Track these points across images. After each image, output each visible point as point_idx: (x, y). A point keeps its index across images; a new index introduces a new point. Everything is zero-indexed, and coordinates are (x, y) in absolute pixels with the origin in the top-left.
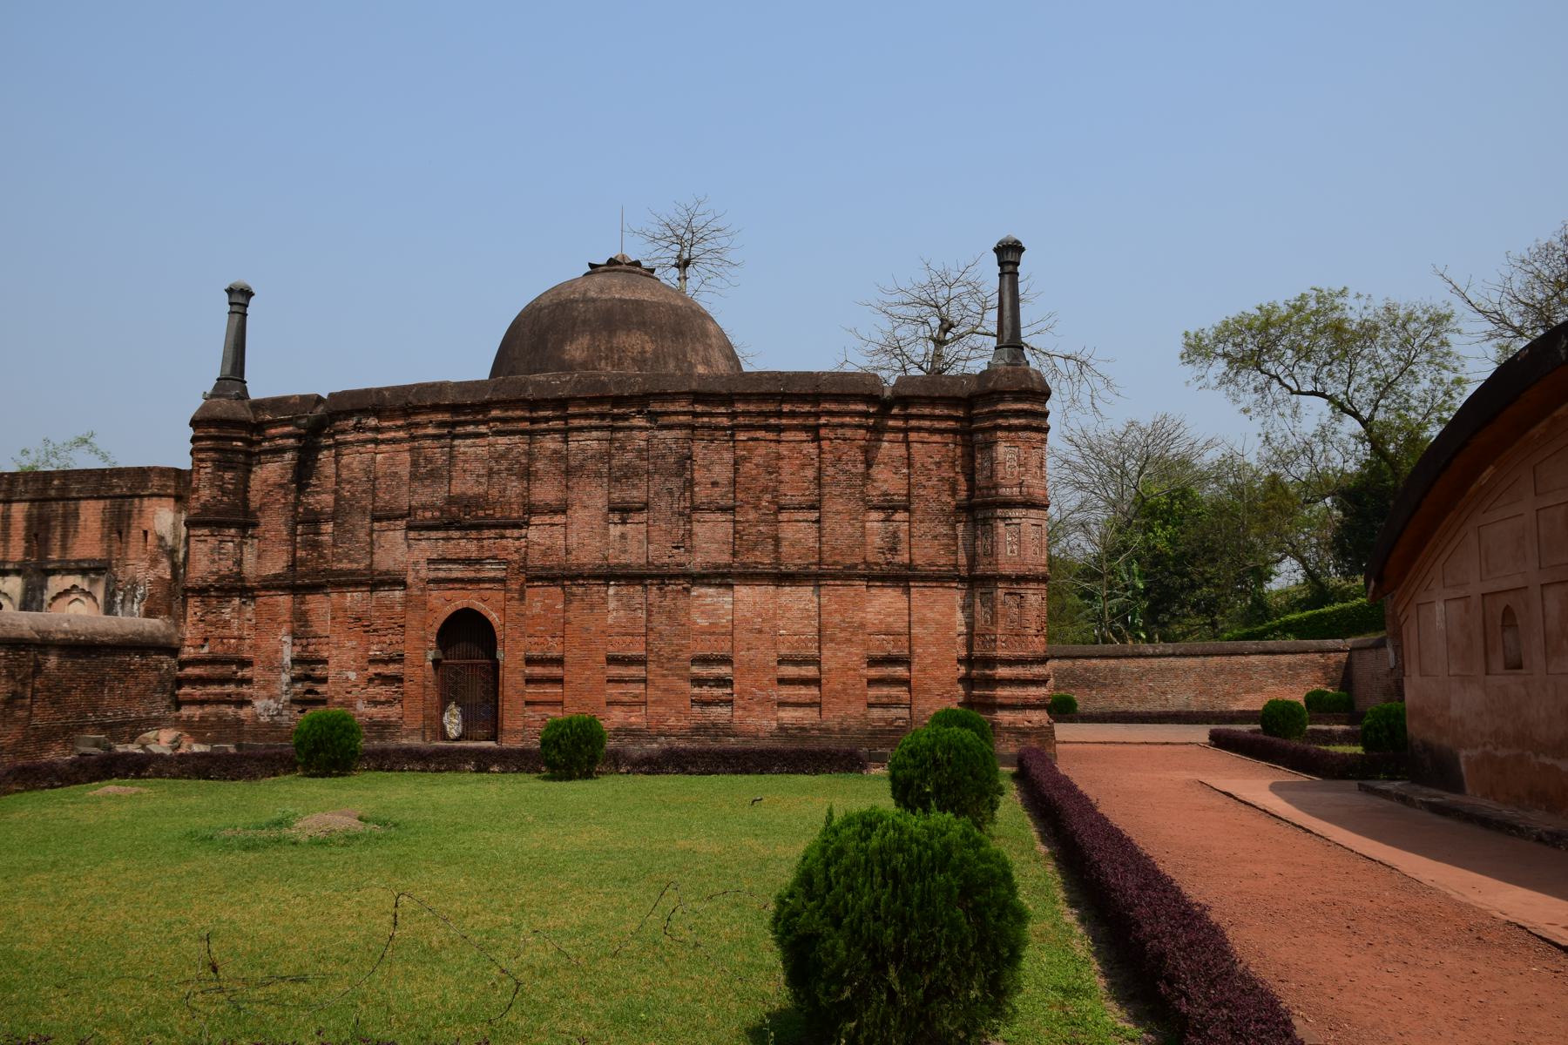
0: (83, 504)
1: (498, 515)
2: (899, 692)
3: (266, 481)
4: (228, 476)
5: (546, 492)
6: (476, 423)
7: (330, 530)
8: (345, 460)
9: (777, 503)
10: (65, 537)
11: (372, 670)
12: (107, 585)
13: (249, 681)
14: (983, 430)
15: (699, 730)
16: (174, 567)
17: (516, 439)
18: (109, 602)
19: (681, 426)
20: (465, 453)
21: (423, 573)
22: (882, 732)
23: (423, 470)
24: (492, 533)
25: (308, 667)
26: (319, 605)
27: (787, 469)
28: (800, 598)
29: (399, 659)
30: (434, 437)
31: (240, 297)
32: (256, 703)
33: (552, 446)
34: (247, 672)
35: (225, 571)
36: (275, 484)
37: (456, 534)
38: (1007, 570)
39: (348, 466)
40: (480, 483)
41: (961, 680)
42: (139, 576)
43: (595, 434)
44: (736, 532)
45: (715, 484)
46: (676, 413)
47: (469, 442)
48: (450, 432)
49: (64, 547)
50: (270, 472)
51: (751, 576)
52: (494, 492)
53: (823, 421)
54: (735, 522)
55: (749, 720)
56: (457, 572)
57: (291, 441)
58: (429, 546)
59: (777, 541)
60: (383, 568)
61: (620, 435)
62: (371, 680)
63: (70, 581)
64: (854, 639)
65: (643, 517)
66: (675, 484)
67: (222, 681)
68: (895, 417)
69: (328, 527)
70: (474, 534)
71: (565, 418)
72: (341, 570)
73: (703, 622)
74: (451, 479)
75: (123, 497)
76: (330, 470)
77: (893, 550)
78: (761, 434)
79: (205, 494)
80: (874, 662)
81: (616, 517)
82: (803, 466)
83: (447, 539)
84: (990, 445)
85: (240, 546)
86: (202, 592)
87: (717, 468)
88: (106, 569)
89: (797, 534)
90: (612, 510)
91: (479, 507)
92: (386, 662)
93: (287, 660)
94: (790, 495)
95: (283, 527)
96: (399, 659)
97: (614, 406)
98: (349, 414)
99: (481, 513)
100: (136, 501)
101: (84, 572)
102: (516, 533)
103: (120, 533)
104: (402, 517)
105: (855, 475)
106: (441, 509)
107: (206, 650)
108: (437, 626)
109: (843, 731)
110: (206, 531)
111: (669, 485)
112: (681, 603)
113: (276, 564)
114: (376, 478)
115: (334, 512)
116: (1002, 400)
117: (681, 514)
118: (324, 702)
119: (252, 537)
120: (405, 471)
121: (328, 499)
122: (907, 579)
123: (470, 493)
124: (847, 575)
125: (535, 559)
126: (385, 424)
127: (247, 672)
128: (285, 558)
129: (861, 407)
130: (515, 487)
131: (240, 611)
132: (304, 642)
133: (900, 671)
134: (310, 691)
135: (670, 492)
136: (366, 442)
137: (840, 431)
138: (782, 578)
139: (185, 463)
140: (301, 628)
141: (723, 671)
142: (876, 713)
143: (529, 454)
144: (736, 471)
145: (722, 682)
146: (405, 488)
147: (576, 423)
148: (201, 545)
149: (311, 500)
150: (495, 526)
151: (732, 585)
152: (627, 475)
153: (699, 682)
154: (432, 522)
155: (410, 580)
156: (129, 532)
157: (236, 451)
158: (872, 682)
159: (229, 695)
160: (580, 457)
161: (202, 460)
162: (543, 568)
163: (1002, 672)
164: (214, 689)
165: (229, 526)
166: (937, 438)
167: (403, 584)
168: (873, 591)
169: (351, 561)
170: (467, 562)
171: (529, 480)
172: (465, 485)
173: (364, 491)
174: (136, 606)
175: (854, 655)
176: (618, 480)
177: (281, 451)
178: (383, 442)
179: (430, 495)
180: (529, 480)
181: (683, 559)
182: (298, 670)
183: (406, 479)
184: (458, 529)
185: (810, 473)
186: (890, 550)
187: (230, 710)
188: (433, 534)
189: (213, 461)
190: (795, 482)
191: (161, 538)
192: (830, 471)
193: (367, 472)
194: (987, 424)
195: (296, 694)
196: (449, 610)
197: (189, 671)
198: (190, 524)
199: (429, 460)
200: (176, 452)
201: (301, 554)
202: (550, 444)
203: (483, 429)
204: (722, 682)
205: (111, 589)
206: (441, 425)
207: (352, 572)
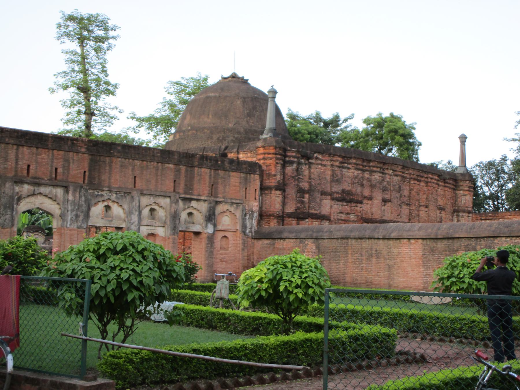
0: (231, 174)
6: (348, 163)
8: (312, 170)
18: (244, 219)
30: (339, 167)
36: (290, 176)
37: (345, 204)
39: (313, 173)
40: (349, 186)
43: (379, 174)
44: (410, 212)
47: (346, 170)
52: (354, 190)
53: (430, 180)
54: (410, 209)
57: (296, 160)
63: (226, 207)
65: (389, 204)
66: (398, 195)
69: (307, 196)
70: (349, 204)
72: (312, 213)
76: (306, 173)
82: (424, 194)
83: (342, 205)
88: (241, 204)
94: (422, 203)
95: (294, 194)
99: (351, 197)
100: (252, 175)
115: (309, 190)
120: (328, 178)
128: (294, 206)
130: (359, 189)
144: (410, 193)
146: (329, 184)
150: (355, 203)
155: (332, 219)
160: (375, 181)
161: (277, 163)
169: (315, 210)
172: (347, 186)
173: (318, 184)
174: (254, 221)
189: (281, 164)
192: (430, 196)
201: (299, 205)
203: (350, 166)
205: (244, 212)
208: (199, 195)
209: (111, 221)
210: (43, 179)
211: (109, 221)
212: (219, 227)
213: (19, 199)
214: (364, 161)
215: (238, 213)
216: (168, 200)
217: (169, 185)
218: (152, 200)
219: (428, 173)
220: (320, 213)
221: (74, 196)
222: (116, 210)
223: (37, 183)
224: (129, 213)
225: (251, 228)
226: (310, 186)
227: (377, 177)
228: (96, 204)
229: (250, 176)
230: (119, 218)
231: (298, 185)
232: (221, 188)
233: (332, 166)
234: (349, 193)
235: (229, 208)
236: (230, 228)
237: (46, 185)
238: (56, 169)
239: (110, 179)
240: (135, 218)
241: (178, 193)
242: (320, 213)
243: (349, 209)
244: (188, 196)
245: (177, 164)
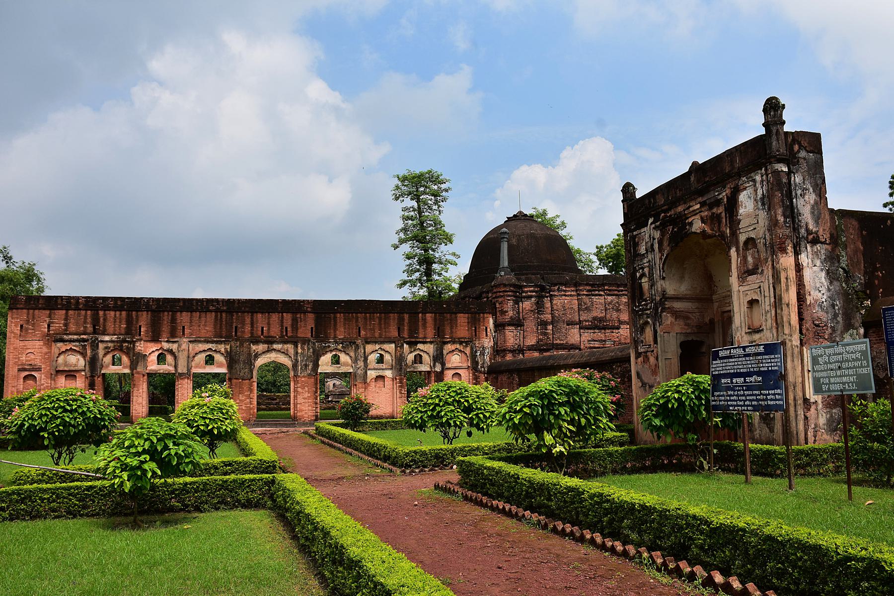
0: (459, 315)
6: (599, 291)
7: (551, 328)
8: (554, 302)
10: (451, 328)
12: (472, 349)
20: (596, 301)
23: (583, 307)
30: (587, 295)
42: (486, 345)
47: (597, 297)
49: (452, 332)
57: (534, 293)
58: (587, 335)
69: (550, 327)
70: (603, 331)
75: (476, 313)
76: (548, 305)
79: (511, 313)
99: (605, 324)
100: (482, 315)
101: (461, 343)
103: (475, 328)
104: (577, 324)
113: (531, 341)
120: (576, 307)
130: (615, 315)
146: (577, 313)
150: (610, 329)
154: (589, 327)
155: (582, 347)
156: (479, 327)
161: (509, 300)
167: (580, 349)
170: (601, 341)
172: (598, 313)
173: (563, 314)
177: (530, 297)
183: (577, 310)
188: (590, 331)
189: (513, 300)
199: (585, 304)
203: (602, 293)
206: (588, 291)
208: (425, 338)
209: (340, 367)
210: (276, 337)
211: (337, 367)
212: (448, 365)
213: (257, 356)
214: (619, 286)
216: (393, 345)
217: (394, 333)
218: (377, 347)
220: (567, 343)
221: (303, 348)
222: (343, 358)
223: (270, 341)
224: (355, 361)
225: (483, 363)
226: (553, 317)
228: (324, 354)
229: (479, 316)
230: (346, 364)
231: (538, 318)
232: (448, 330)
233: (578, 295)
234: (601, 320)
235: (458, 346)
236: (461, 365)
237: (278, 343)
238: (286, 328)
239: (335, 331)
240: (361, 364)
241: (403, 337)
242: (567, 343)
243: (602, 336)
244: (414, 340)
245: (401, 313)
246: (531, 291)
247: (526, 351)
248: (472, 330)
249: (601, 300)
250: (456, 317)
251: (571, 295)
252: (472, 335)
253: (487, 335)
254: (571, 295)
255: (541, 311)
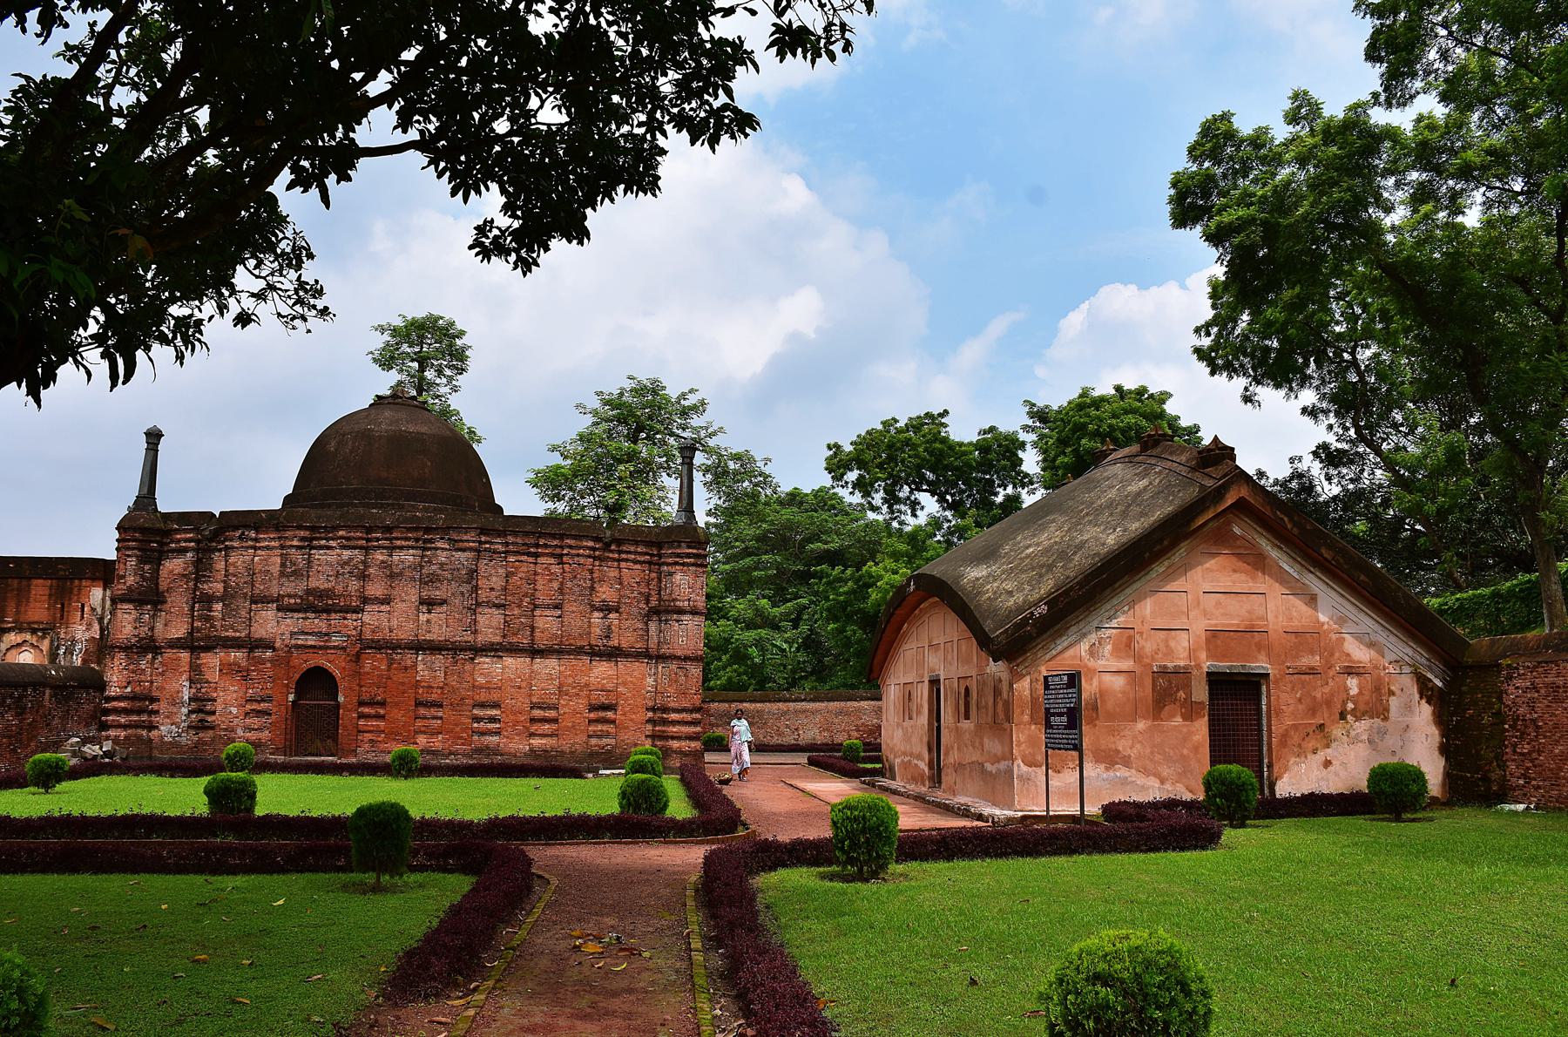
1: (342, 604)
2: (610, 728)
3: (172, 571)
4: (147, 567)
5: (375, 589)
6: (328, 539)
7: (219, 609)
9: (534, 604)
10: (18, 606)
11: (248, 707)
12: (52, 642)
13: (157, 712)
14: (668, 564)
15: (479, 751)
16: (102, 630)
17: (356, 552)
19: (471, 549)
20: (319, 559)
21: (287, 641)
22: (597, 753)
23: (289, 570)
24: (338, 616)
25: (201, 704)
26: (212, 661)
27: (541, 582)
28: (549, 667)
29: (267, 699)
31: (154, 437)
32: (162, 728)
33: (381, 558)
34: (154, 706)
35: (143, 635)
38: (679, 653)
41: (649, 721)
42: (78, 636)
45: (492, 589)
46: (467, 541)
47: (321, 552)
48: (309, 545)
49: (18, 612)
50: (174, 566)
51: (514, 650)
52: (339, 588)
53: (565, 552)
54: (506, 615)
55: (511, 745)
56: (311, 641)
58: (292, 622)
59: (533, 628)
60: (257, 636)
61: (429, 553)
62: (247, 714)
64: (581, 693)
65: (444, 608)
66: (465, 588)
67: (139, 712)
68: (612, 551)
69: (218, 606)
70: (325, 616)
71: (390, 539)
73: (481, 680)
74: (308, 576)
75: (66, 578)
77: (608, 637)
78: (524, 558)
79: (131, 580)
80: (593, 708)
81: (424, 609)
82: (551, 581)
84: (671, 574)
85: (153, 617)
86: (127, 649)
87: (494, 579)
89: (547, 623)
90: (421, 603)
91: (329, 597)
92: (259, 702)
93: (186, 698)
94: (542, 599)
96: (267, 699)
97: (424, 534)
98: (236, 528)
99: (330, 602)
100: (77, 582)
101: (34, 631)
102: (354, 616)
103: (63, 605)
104: (273, 602)
105: (585, 588)
106: (301, 597)
107: (129, 689)
108: (297, 676)
109: (571, 752)
110: (131, 607)
111: (461, 589)
112: (468, 667)
113: (179, 631)
114: (254, 574)
116: (679, 547)
117: (469, 609)
118: (212, 728)
119: (161, 610)
120: (275, 570)
121: (220, 586)
122: (617, 656)
123: (322, 587)
124: (579, 651)
125: (368, 635)
126: (262, 536)
127: (154, 706)
129: (590, 544)
130: (354, 585)
131: (153, 663)
132: (199, 686)
133: (610, 714)
134: (201, 721)
135: (462, 593)
136: (248, 548)
137: (576, 559)
138: (534, 652)
139: (111, 555)
140: (195, 679)
141: (494, 712)
142: (594, 741)
143: (364, 562)
145: (492, 720)
146: (275, 582)
147: (398, 543)
148: (126, 616)
149: (206, 587)
150: (340, 611)
151: (502, 657)
152: (433, 580)
153: (478, 719)
155: (277, 645)
157: (153, 550)
158: (591, 721)
159: (144, 721)
160: (401, 567)
161: (129, 556)
162: (372, 640)
163: (674, 716)
164: (135, 718)
165: (147, 604)
166: (638, 566)
167: (274, 649)
168: (594, 663)
169: (235, 631)
170: (319, 634)
171: (364, 581)
173: (245, 583)
174: (75, 657)
175: (581, 704)
176: (426, 583)
177: (184, 551)
178: (259, 548)
179: (299, 587)
180: (364, 581)
181: (470, 639)
182: (194, 705)
184: (313, 612)
185: (556, 585)
186: (606, 637)
187: (144, 733)
188: (296, 615)
189: (137, 556)
190: (545, 590)
191: (93, 610)
192: (569, 584)
193: (248, 569)
194: (670, 560)
195: (192, 722)
196: (305, 667)
197: (115, 704)
198: (114, 601)
200: (104, 547)
202: (380, 556)
203: (333, 543)
204: (492, 720)
206: (302, 539)
207: (234, 638)
215: (45, 645)
219: (562, 537)
227: (408, 557)
229: (72, 583)
235: (28, 637)
246: (186, 540)
247: (166, 648)
248: (55, 608)
249: (331, 557)
250: (29, 586)
251: (267, 548)
252: (55, 619)
253: (82, 617)
254: (267, 548)
255: (204, 576)
